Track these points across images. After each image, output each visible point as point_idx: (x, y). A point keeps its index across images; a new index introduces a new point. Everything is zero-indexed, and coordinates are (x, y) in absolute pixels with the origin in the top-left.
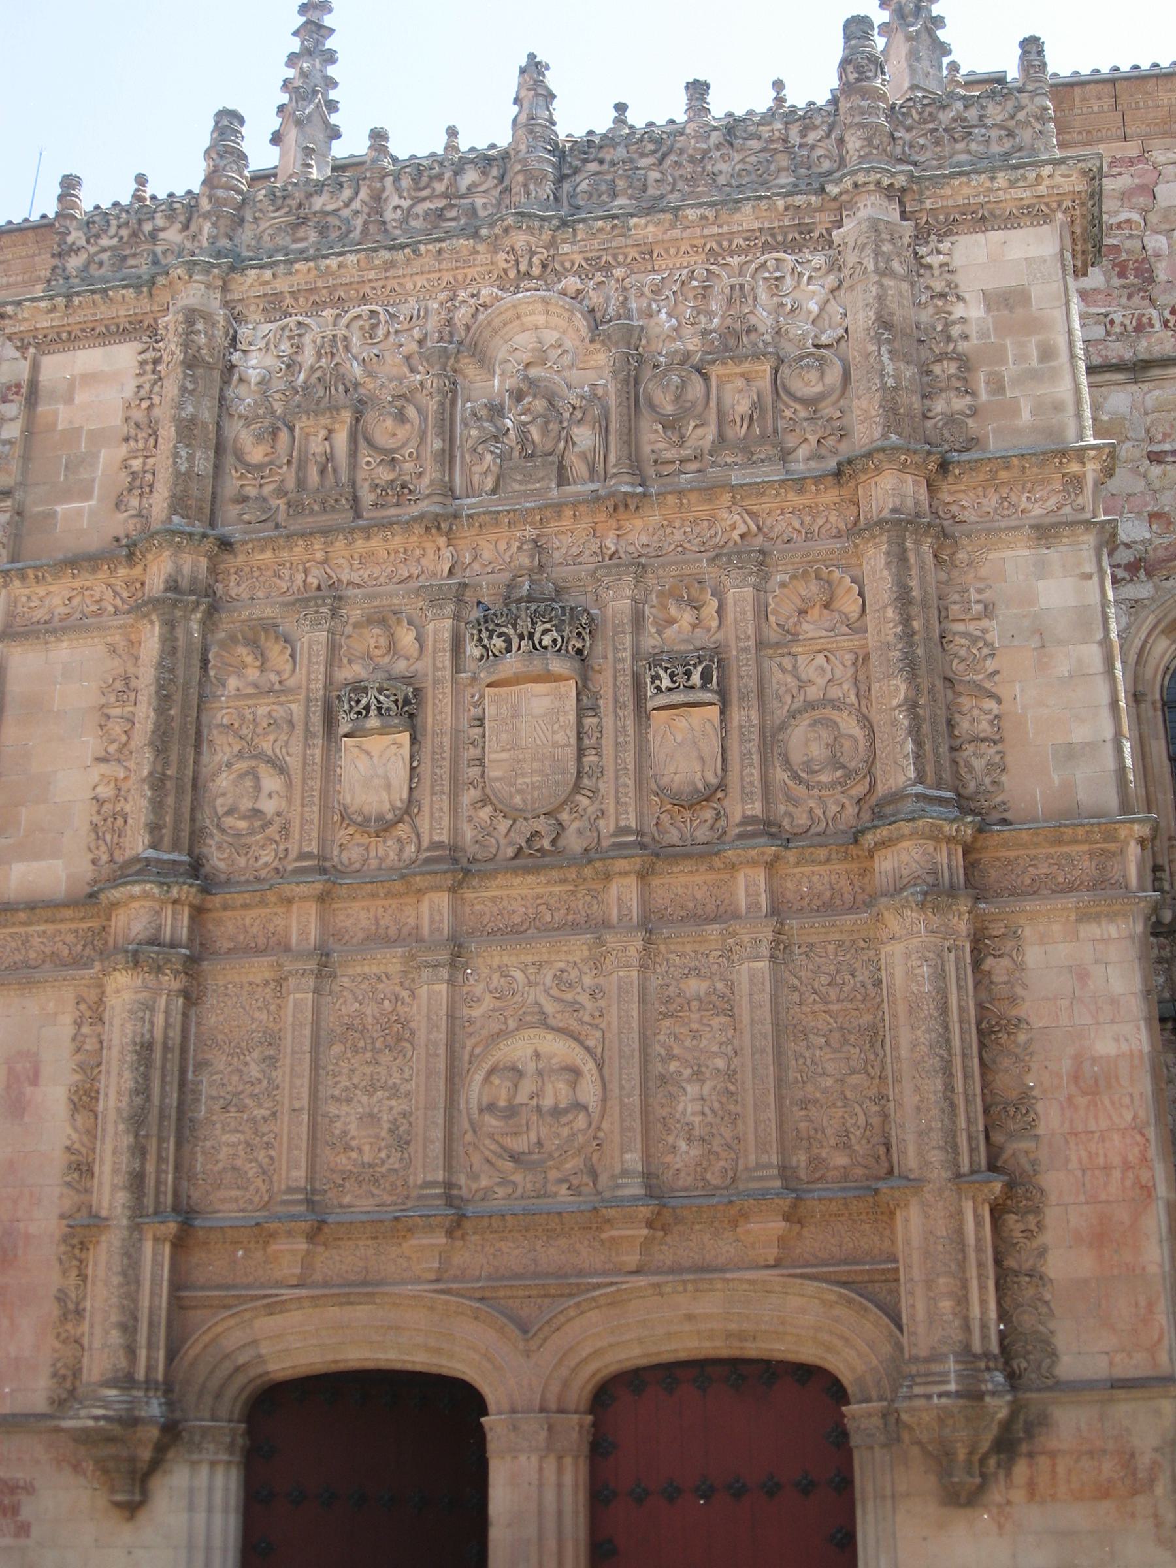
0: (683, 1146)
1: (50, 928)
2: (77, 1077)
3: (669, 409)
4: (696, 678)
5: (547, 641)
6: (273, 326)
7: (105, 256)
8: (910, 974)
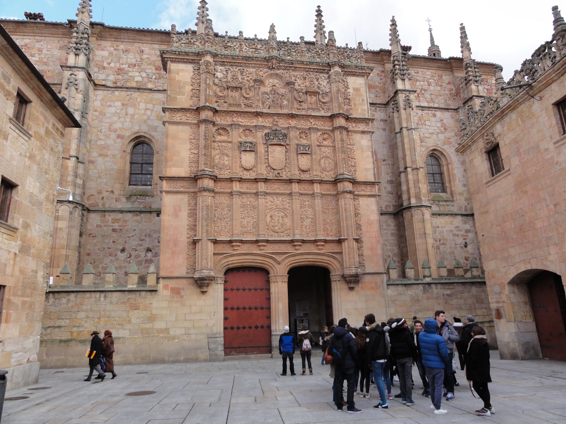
0: (305, 230)
1: (182, 181)
2: (190, 211)
3: (300, 100)
4: (307, 149)
5: (281, 138)
6: (223, 68)
7: (183, 45)
8: (345, 204)
